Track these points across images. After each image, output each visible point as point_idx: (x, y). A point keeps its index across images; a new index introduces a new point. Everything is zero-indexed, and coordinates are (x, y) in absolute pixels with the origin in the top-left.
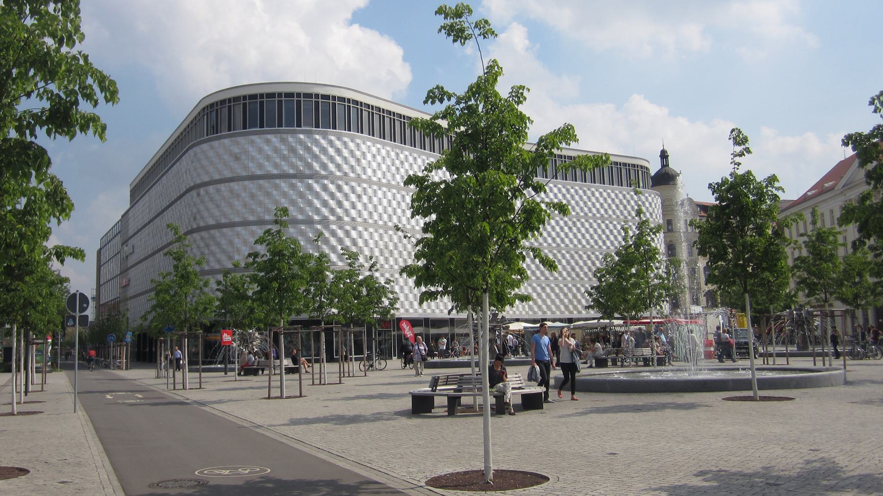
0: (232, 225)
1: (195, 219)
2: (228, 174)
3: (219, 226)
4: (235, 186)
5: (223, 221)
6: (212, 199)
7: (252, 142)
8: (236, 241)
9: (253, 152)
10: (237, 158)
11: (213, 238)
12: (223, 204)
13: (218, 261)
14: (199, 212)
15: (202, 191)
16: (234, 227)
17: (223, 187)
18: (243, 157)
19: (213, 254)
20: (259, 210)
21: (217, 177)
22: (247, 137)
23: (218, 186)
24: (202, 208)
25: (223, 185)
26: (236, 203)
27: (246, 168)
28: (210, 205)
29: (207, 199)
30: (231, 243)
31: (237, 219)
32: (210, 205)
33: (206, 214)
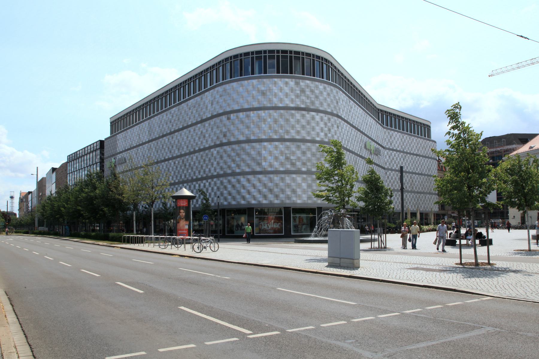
0: (260, 141)
1: (225, 136)
2: (256, 105)
3: (248, 141)
4: (262, 113)
5: (252, 138)
6: (242, 122)
7: (275, 83)
8: (264, 152)
9: (275, 90)
10: (263, 94)
11: (243, 149)
12: (252, 126)
13: (248, 166)
14: (229, 130)
15: (232, 116)
16: (262, 142)
17: (252, 114)
18: (268, 93)
19: (243, 160)
20: (281, 131)
21: (246, 106)
22: (271, 79)
23: (248, 113)
24: (232, 128)
25: (251, 112)
26: (264, 126)
27: (270, 101)
28: (241, 126)
29: (236, 122)
30: (259, 154)
31: (264, 137)
32: (241, 126)
33: (236, 133)
